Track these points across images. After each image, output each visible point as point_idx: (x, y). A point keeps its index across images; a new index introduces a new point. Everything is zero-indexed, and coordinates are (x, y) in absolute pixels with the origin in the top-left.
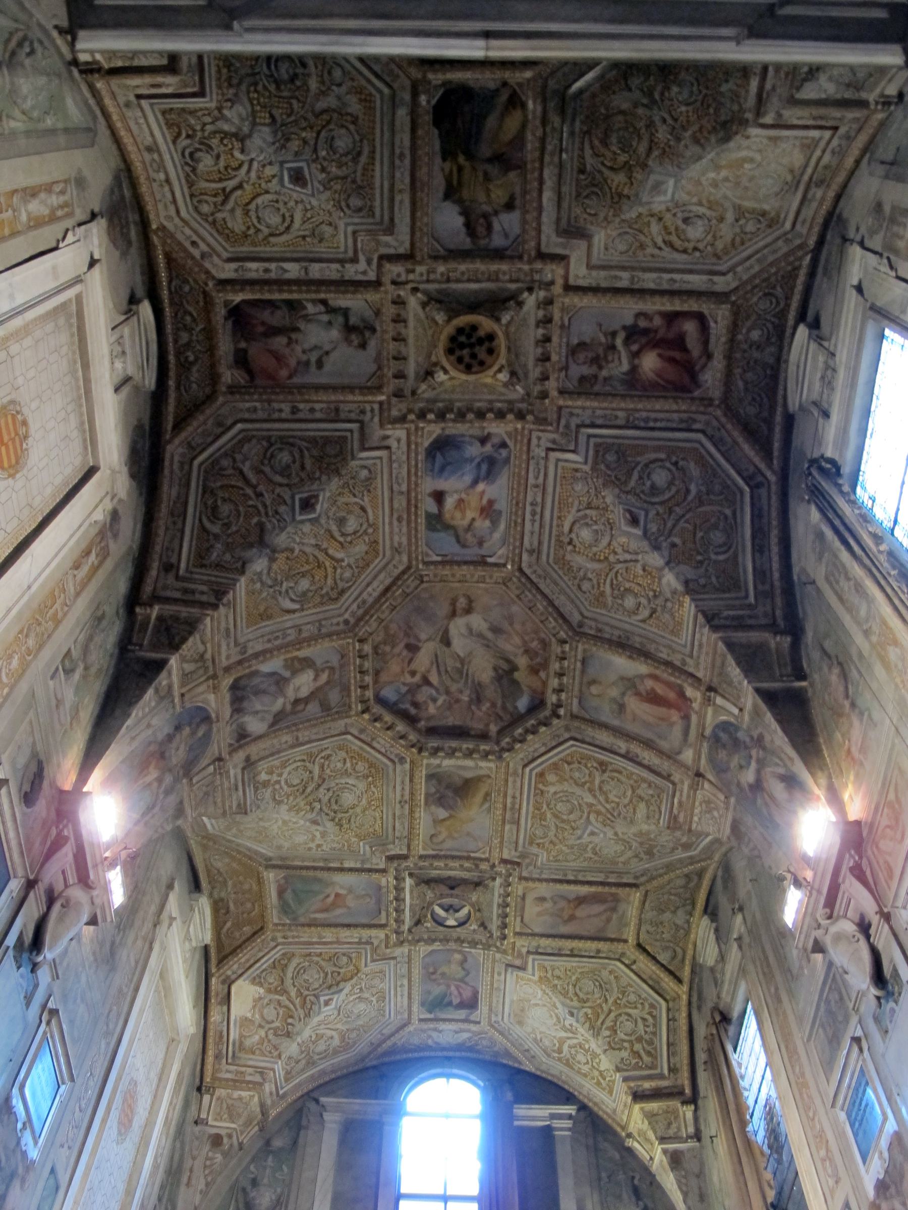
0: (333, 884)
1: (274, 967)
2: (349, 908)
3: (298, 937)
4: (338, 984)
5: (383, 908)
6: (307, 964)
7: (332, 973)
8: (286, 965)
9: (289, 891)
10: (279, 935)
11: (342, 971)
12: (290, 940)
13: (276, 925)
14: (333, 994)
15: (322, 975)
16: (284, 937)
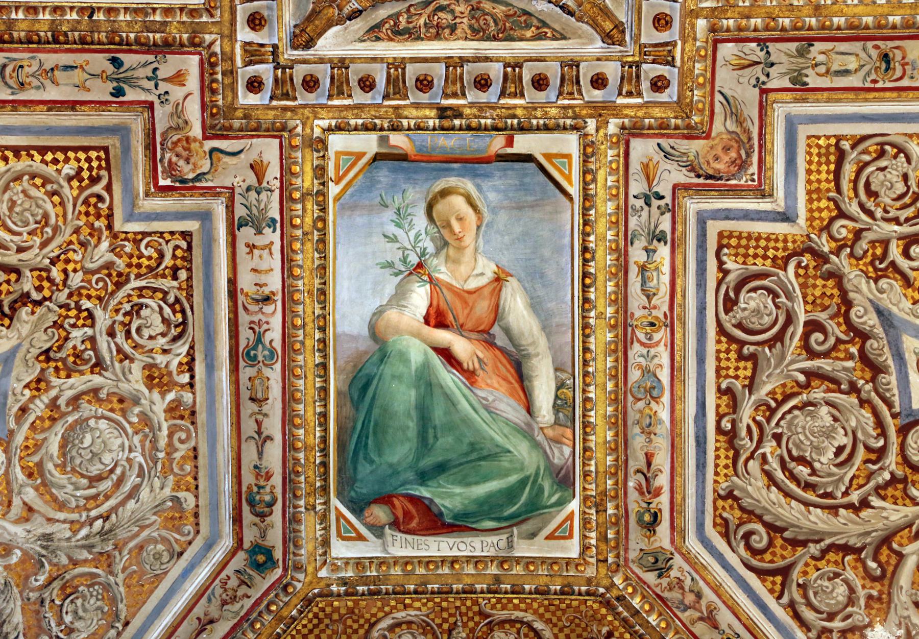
0: (374, 333)
1: (785, 572)
2: (498, 280)
3: (648, 471)
4: (863, 336)
5: (497, 144)
6: (769, 447)
7: (812, 354)
8: (773, 528)
9: (424, 492)
10: (637, 541)
11: (802, 318)
12: (664, 501)
13: (585, 548)
14: (899, 357)
15: (818, 394)
16: (651, 526)
